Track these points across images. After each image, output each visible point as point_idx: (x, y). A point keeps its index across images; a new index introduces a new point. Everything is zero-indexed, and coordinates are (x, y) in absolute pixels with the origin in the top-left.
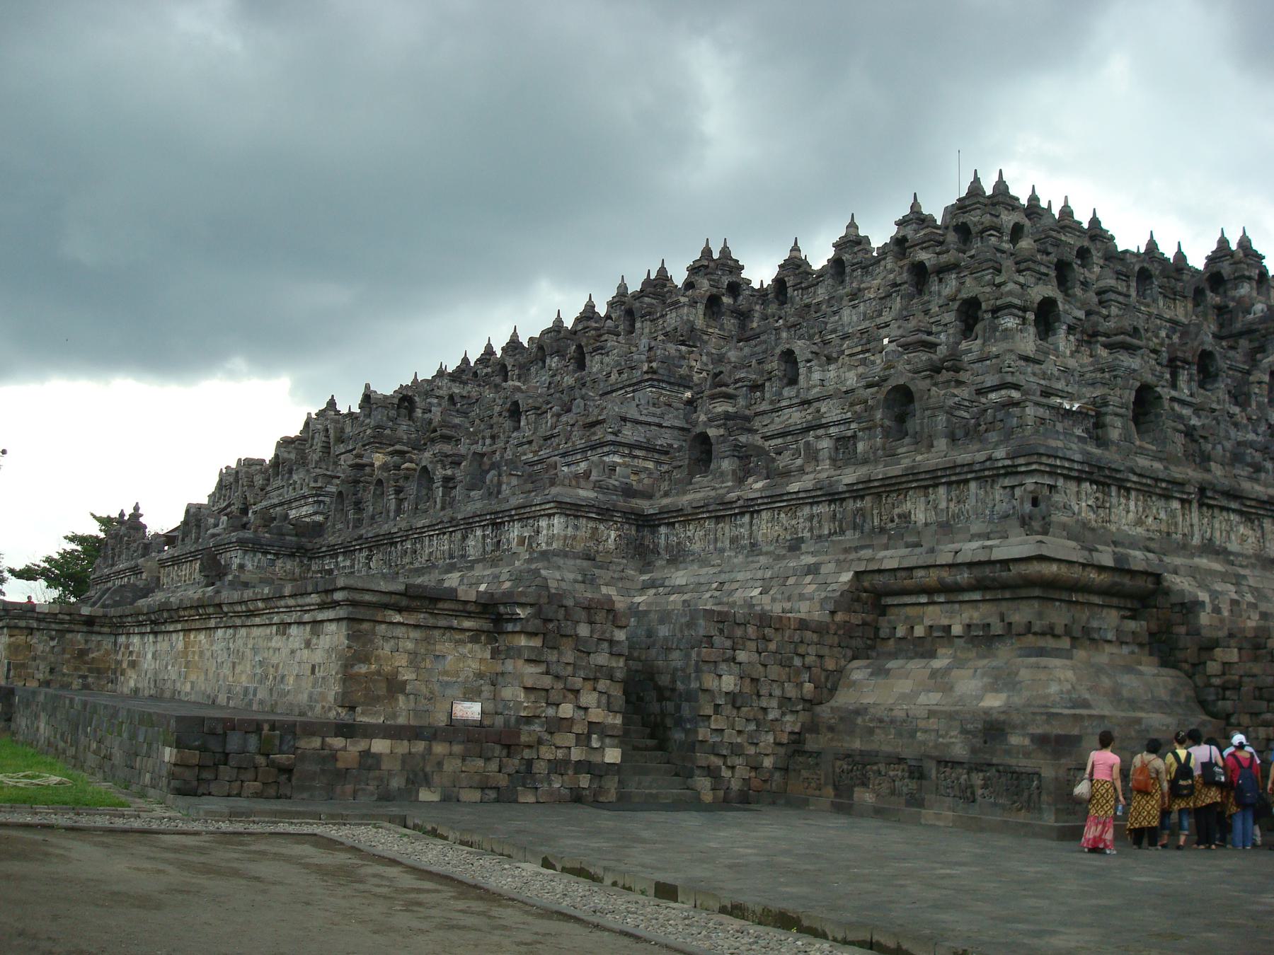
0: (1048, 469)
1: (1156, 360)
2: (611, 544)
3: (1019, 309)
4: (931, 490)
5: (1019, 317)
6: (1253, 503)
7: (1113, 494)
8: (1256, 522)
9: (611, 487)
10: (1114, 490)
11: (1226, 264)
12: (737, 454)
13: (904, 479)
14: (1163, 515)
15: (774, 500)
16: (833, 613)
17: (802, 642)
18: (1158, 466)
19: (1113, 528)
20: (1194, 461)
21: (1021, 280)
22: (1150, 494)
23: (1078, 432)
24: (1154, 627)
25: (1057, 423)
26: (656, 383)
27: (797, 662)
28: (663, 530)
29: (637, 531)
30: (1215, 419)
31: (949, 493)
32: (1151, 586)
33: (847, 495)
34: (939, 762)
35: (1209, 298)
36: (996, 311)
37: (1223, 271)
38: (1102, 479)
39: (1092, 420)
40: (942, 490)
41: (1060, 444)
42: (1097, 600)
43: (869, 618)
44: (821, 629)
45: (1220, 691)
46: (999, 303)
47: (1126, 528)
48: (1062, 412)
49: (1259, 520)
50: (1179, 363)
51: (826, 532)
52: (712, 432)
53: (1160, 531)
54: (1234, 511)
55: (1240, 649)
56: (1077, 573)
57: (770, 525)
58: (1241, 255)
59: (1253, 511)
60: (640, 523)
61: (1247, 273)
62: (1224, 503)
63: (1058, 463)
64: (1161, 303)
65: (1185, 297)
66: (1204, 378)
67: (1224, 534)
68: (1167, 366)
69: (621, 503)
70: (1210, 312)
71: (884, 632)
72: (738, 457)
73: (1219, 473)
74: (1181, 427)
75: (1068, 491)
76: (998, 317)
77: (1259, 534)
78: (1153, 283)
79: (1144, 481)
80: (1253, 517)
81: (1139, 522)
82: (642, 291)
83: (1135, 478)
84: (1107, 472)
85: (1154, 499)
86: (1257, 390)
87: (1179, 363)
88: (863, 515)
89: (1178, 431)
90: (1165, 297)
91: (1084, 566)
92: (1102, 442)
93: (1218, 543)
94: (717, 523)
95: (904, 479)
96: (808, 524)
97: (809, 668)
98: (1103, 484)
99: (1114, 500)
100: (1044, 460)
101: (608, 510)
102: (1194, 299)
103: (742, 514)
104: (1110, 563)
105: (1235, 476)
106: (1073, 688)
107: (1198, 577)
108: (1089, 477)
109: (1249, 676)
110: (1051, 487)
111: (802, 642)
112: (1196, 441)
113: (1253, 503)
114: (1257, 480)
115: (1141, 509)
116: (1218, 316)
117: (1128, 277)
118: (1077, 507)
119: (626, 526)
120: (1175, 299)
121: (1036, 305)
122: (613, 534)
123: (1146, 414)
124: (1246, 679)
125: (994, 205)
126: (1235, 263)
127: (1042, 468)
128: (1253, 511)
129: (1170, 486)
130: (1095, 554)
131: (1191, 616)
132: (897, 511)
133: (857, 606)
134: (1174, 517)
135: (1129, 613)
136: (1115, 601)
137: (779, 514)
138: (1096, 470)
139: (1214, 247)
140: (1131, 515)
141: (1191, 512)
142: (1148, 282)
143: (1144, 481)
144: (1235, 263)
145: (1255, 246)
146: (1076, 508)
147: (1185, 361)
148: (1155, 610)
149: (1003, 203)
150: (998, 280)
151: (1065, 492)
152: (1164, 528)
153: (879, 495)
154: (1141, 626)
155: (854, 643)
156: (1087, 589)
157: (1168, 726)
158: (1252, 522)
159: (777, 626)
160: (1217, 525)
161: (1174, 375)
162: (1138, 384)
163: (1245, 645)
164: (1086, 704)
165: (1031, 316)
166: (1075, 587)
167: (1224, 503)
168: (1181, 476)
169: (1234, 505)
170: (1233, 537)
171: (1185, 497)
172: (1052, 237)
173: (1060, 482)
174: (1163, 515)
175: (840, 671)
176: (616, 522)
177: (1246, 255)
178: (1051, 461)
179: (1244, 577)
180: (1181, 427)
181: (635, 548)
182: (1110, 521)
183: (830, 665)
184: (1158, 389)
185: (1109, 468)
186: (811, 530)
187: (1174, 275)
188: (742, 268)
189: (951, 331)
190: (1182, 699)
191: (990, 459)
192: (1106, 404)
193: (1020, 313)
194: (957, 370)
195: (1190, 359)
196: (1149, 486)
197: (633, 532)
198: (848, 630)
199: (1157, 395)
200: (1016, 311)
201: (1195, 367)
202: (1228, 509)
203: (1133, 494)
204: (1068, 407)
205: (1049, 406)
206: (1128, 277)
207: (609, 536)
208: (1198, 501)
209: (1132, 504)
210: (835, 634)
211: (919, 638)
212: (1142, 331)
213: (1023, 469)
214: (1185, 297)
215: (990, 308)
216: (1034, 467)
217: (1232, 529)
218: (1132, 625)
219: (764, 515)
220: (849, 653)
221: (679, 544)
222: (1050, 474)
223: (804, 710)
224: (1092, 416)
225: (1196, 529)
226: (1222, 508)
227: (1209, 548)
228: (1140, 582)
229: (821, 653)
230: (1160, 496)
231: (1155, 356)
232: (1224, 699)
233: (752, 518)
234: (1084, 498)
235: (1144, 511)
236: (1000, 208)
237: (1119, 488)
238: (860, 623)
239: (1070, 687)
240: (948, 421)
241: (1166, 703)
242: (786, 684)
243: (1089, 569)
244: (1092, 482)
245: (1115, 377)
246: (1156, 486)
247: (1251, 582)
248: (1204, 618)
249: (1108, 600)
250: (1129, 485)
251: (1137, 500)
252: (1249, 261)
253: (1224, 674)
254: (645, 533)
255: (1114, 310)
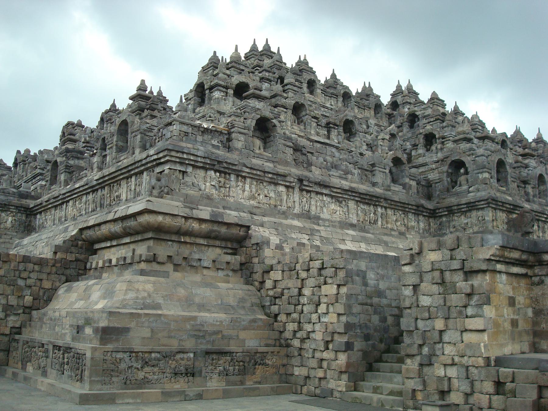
0: (178, 160)
1: (317, 123)
2: (9, 224)
3: (223, 87)
4: (129, 180)
5: (223, 92)
6: (338, 191)
7: (232, 179)
8: (344, 203)
9: (11, 192)
10: (233, 177)
11: (400, 97)
12: (67, 171)
13: (117, 174)
14: (272, 195)
15: (72, 193)
16: (55, 253)
17: (25, 270)
18: (271, 165)
19: (232, 200)
20: (303, 166)
21: (228, 72)
22: (262, 182)
23: (215, 142)
24: (243, 260)
25: (198, 136)
26: (89, 148)
27: (21, 282)
28: (38, 216)
29: (27, 217)
30: (352, 156)
31: (136, 180)
32: (242, 233)
33: (98, 187)
34: (54, 346)
35: (383, 110)
36: (211, 88)
37: (398, 100)
38: (222, 169)
39: (226, 137)
40: (133, 179)
41: (190, 146)
42: (202, 241)
43: (82, 257)
44: (41, 262)
45: (273, 299)
46: (212, 84)
47: (242, 201)
48: (202, 130)
49: (345, 202)
50: (331, 125)
51: (90, 210)
52: (59, 160)
53: (270, 205)
54: (326, 195)
55: (283, 271)
56: (179, 222)
57: (72, 208)
58: (407, 92)
59: (340, 195)
60: (28, 213)
61: (408, 101)
62: (318, 189)
63: (185, 156)
64: (356, 111)
65: (370, 108)
66: (350, 135)
67: (319, 208)
68: (325, 127)
69: (15, 201)
70: (384, 116)
71: (88, 266)
72: (69, 173)
73: (317, 173)
74: (291, 144)
75: (197, 176)
76: (212, 92)
77: (345, 209)
78: (351, 100)
79: (255, 172)
80: (341, 199)
81: (253, 197)
82: (110, 109)
83: (248, 170)
84: (225, 165)
85: (265, 184)
86: (382, 143)
87: (331, 125)
88: (104, 198)
89: (288, 146)
90: (359, 107)
91: (186, 218)
92: (229, 149)
93: (313, 213)
94: (56, 210)
95: (117, 174)
96: (84, 207)
97: (30, 287)
98: (225, 173)
99: (233, 183)
100: (173, 154)
101: (5, 205)
102: (375, 110)
103: (62, 203)
104: (208, 217)
105: (330, 175)
106: (149, 295)
107: (280, 229)
108: (212, 167)
109: (287, 289)
110: (184, 173)
111: (25, 270)
112: (305, 155)
113: (338, 191)
114: (346, 179)
115: (254, 190)
116: (389, 119)
117: (337, 96)
118: (204, 186)
119: (19, 215)
120: (364, 109)
121: (234, 86)
122: (10, 219)
123: (269, 137)
124: (286, 291)
125: (261, 55)
126: (404, 96)
127: (173, 159)
128: (340, 195)
129: (275, 177)
130: (194, 211)
131: (261, 251)
132: (117, 194)
133: (73, 249)
134: (280, 196)
135: (230, 251)
136: (218, 243)
137: (76, 202)
138: (216, 163)
139: (394, 89)
140: (246, 193)
141: (294, 194)
142: (349, 100)
143: (255, 172)
144: (404, 96)
145: (414, 89)
146: (203, 187)
147: (335, 124)
148: (245, 249)
149: (266, 54)
150: (215, 72)
151: (195, 176)
152: (272, 202)
153: (109, 185)
154: (235, 259)
155: (68, 272)
156: (189, 233)
157: (221, 322)
158: (341, 202)
159: (5, 260)
160: (313, 202)
161: (329, 132)
162: (259, 117)
163: (286, 268)
164: (158, 306)
165: (231, 92)
166: (179, 232)
167: (318, 189)
168: (283, 171)
169: (325, 191)
170: (325, 210)
171: (288, 184)
172: (277, 65)
173: (190, 169)
174: (272, 195)
175: (55, 290)
176: (12, 212)
177: (409, 93)
178: (179, 155)
179: (318, 231)
180: (291, 144)
181: (25, 227)
182: (229, 196)
183: (47, 285)
184: (274, 121)
185: (226, 162)
186: (85, 209)
187: (365, 97)
188: (168, 101)
189: (192, 103)
190: (248, 305)
191: (148, 156)
192: (233, 126)
193: (224, 90)
194: (153, 110)
195: (338, 123)
196: (259, 176)
197: (24, 218)
198: (65, 265)
199: (273, 124)
200: (221, 88)
201: (342, 128)
202: (322, 194)
203: (248, 180)
204: (205, 127)
205: (192, 126)
206: (337, 96)
207: (7, 219)
208: (299, 188)
209: (247, 187)
210: (54, 266)
211: (102, 268)
212: (307, 106)
213: (162, 160)
214: (370, 108)
215: (208, 87)
216: (167, 158)
217: (325, 206)
218: (228, 258)
219: (71, 203)
220: (64, 278)
221: (42, 223)
222: (181, 163)
223: (23, 313)
224: (226, 134)
225: (297, 204)
226: (317, 193)
227: (306, 216)
228: (234, 231)
229: (41, 277)
230: (270, 183)
231: (316, 121)
232: (275, 304)
233: (67, 206)
234: (209, 180)
235: (257, 191)
236: (264, 57)
237: (238, 176)
238: (74, 259)
239: (146, 295)
240: (142, 138)
241: (232, 307)
242: (9, 297)
243: (191, 221)
244: (216, 171)
245: (245, 112)
246: (265, 176)
247: (323, 234)
248: (267, 252)
249: (211, 242)
250: (244, 174)
251: (251, 184)
252: (410, 95)
253: (275, 287)
254: (32, 219)
255: (290, 94)
